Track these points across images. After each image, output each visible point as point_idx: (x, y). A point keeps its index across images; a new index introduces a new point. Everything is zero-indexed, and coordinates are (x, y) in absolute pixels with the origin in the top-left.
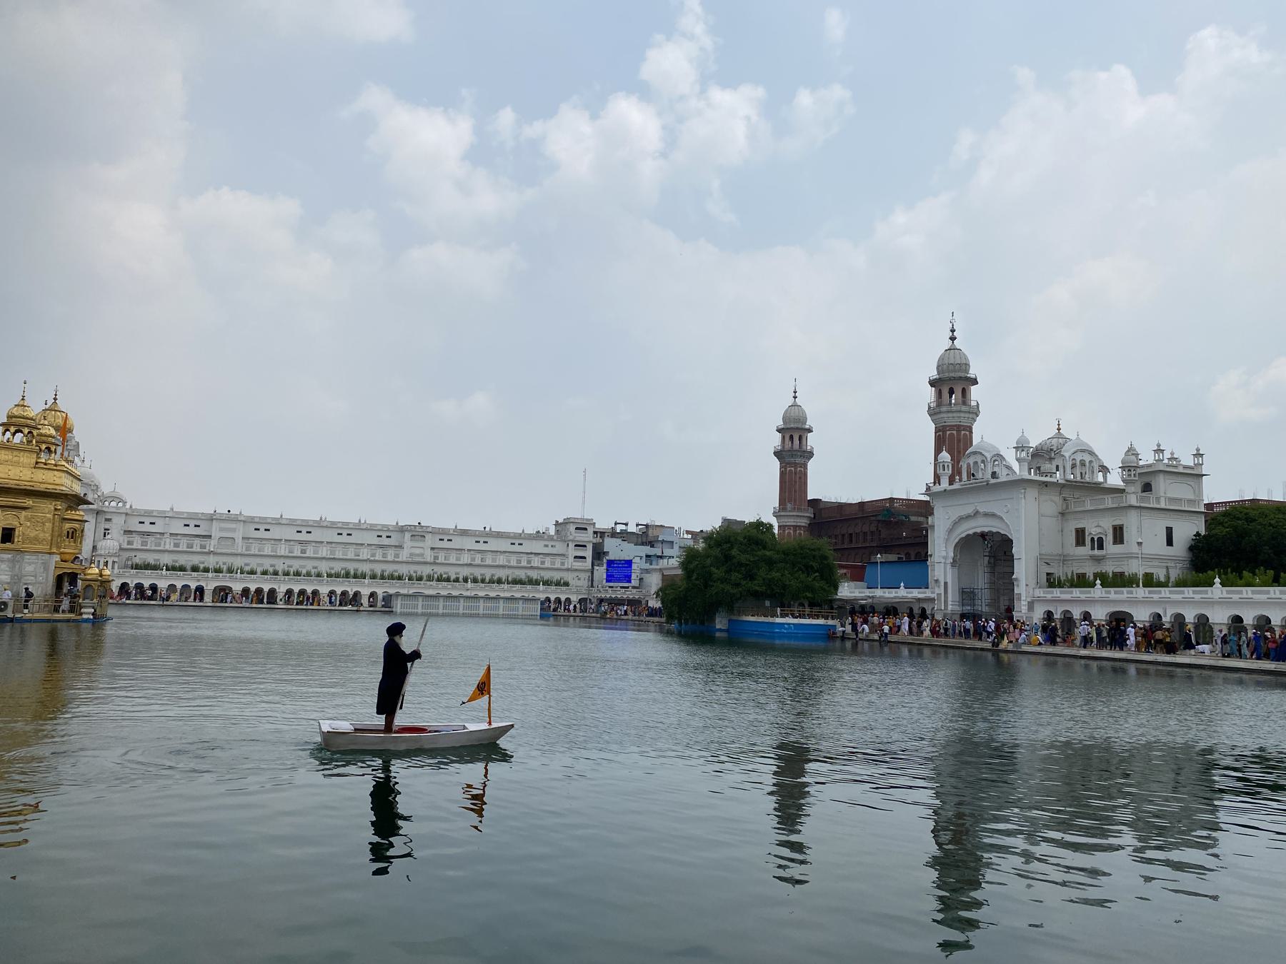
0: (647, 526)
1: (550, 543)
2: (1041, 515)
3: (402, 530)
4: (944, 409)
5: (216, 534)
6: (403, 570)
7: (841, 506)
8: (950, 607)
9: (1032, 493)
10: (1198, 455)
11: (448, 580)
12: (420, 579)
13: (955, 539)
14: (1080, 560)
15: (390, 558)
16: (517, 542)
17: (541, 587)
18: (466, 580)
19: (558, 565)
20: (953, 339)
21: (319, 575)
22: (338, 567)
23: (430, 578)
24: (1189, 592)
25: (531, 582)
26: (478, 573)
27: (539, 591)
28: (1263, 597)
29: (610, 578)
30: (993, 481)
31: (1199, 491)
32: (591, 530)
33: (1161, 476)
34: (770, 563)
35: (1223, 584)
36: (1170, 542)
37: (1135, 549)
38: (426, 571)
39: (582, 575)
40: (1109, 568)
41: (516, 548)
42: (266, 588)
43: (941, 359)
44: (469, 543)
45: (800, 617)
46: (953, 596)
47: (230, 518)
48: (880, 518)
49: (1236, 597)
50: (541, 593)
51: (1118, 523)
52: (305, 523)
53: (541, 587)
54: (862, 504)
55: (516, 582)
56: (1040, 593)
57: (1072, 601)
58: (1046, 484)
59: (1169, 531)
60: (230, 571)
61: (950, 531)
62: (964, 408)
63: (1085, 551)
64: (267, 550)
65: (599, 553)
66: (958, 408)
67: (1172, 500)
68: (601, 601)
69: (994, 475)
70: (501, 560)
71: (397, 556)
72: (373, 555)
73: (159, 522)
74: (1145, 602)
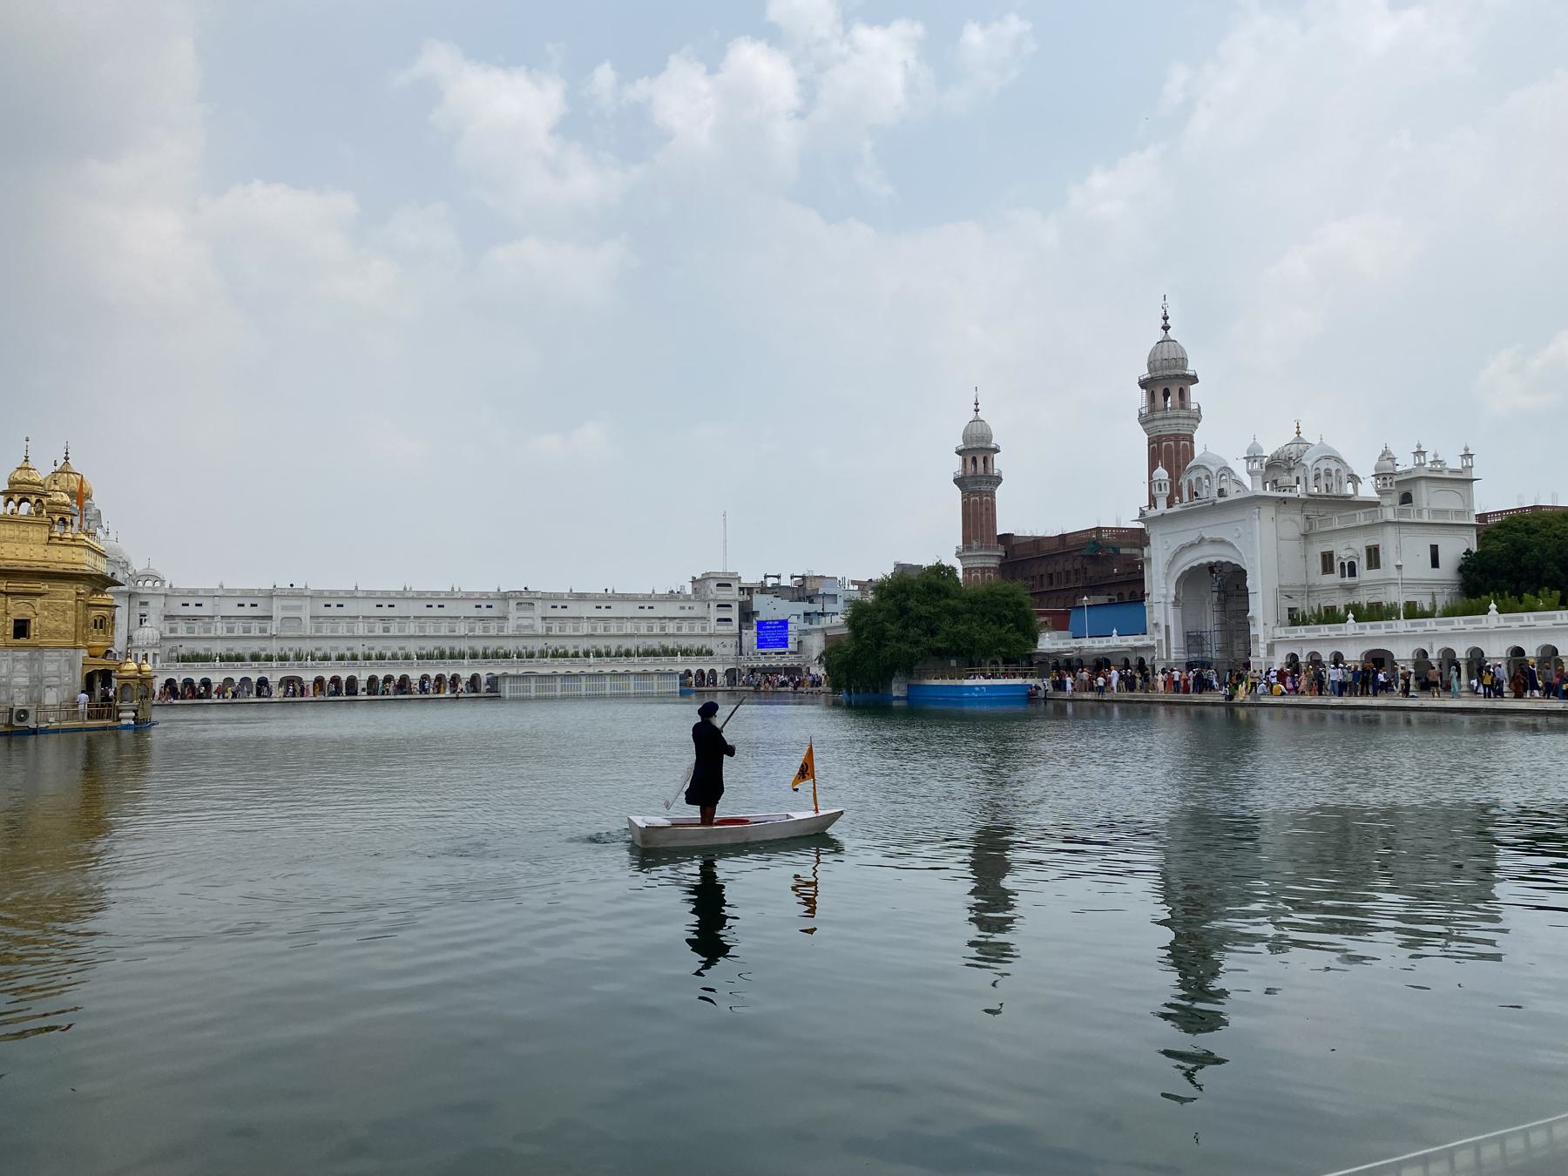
0: (804, 577)
1: (687, 605)
2: (1279, 539)
3: (505, 597)
4: (1158, 415)
5: (277, 613)
6: (510, 646)
7: (1037, 541)
8: (1173, 656)
9: (1268, 512)
10: (1468, 455)
11: (565, 655)
12: (531, 655)
13: (1177, 573)
14: (1330, 590)
15: (493, 632)
16: (647, 605)
17: (679, 658)
18: (587, 654)
19: (698, 631)
20: (1166, 328)
21: (407, 657)
22: (429, 646)
23: (543, 654)
24: (1459, 622)
25: (666, 652)
26: (601, 645)
27: (676, 663)
28: (1548, 623)
29: (762, 643)
30: (1222, 500)
31: (1469, 499)
32: (735, 586)
33: (1423, 483)
34: (955, 614)
35: (1500, 611)
36: (1435, 563)
37: (1394, 574)
38: (538, 645)
39: (728, 641)
40: (1364, 599)
41: (646, 613)
42: (344, 677)
43: (1153, 354)
44: (588, 610)
45: (993, 676)
46: (1176, 641)
48: (1085, 552)
49: (1515, 625)
50: (680, 665)
51: (1371, 543)
52: (386, 595)
53: (679, 658)
54: (1063, 537)
55: (647, 653)
56: (1280, 632)
57: (1319, 641)
58: (1284, 501)
59: (1434, 550)
60: (298, 658)
61: (1171, 563)
62: (1183, 413)
63: (1335, 578)
64: (342, 630)
65: (747, 614)
66: (1175, 413)
67: (1436, 512)
68: (753, 671)
69: (1221, 493)
70: (629, 628)
71: (501, 629)
72: (472, 630)
73: (207, 603)
74: (1408, 637)
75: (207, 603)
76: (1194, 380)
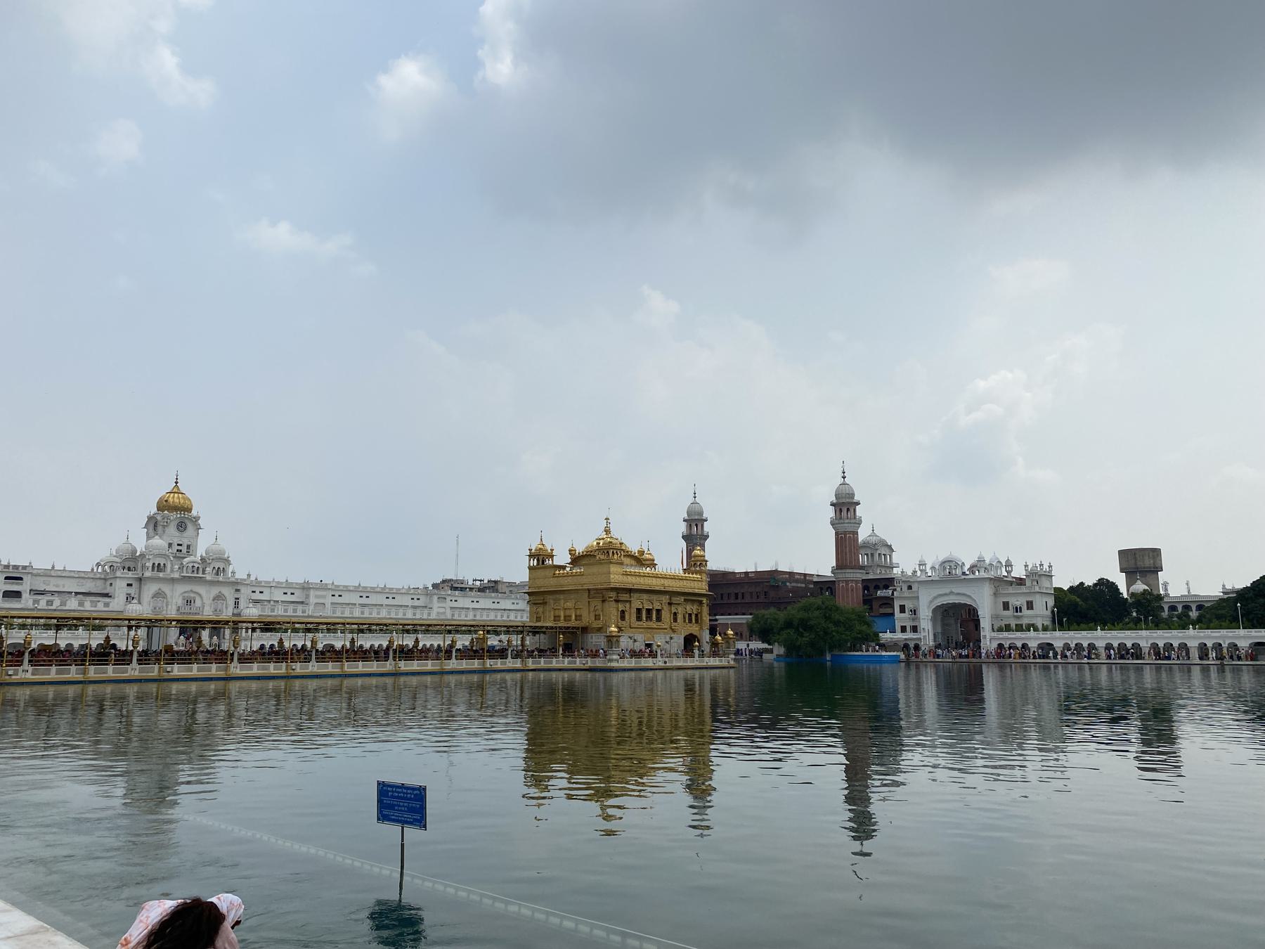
7: (725, 574)
10: (1050, 566)
40: (1025, 622)
46: (931, 637)
47: (322, 587)
54: (746, 573)
57: (1018, 638)
63: (1010, 613)
73: (266, 591)
75: (266, 591)
76: (858, 504)
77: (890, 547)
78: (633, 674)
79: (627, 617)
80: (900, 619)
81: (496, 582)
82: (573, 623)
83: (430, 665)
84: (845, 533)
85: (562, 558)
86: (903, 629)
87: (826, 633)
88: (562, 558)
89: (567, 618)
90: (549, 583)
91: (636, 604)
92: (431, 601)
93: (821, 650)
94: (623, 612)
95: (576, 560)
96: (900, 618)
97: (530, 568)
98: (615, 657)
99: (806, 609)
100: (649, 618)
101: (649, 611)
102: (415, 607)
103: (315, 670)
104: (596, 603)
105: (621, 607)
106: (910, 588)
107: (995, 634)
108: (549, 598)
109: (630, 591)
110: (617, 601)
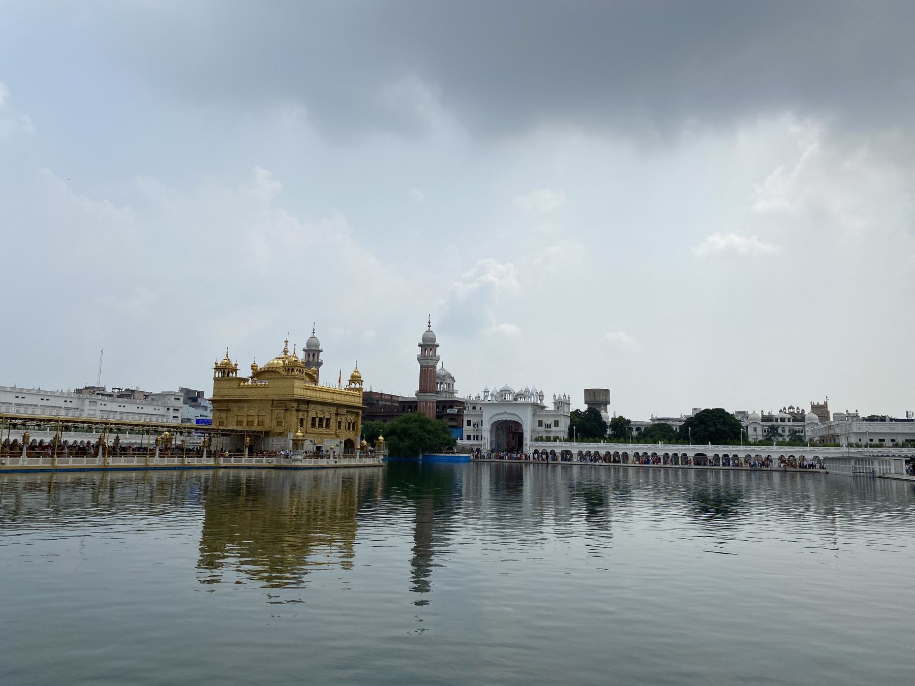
40: (552, 435)
57: (548, 446)
76: (438, 346)
77: (453, 378)
78: (312, 472)
79: (305, 422)
80: (467, 430)
81: (133, 391)
82: (255, 428)
83: (135, 462)
84: (428, 367)
85: (245, 372)
86: (469, 438)
87: (421, 440)
88: (245, 372)
89: (250, 423)
90: (233, 392)
91: (312, 414)
92: (83, 404)
93: (420, 450)
94: (302, 420)
95: (258, 374)
96: (467, 430)
97: (215, 379)
98: (300, 457)
99: (407, 421)
100: (321, 425)
101: (321, 419)
102: (66, 408)
103: (26, 464)
104: (279, 412)
105: (301, 415)
106: (474, 408)
107: (533, 443)
108: (234, 407)
109: (308, 402)
110: (298, 410)
